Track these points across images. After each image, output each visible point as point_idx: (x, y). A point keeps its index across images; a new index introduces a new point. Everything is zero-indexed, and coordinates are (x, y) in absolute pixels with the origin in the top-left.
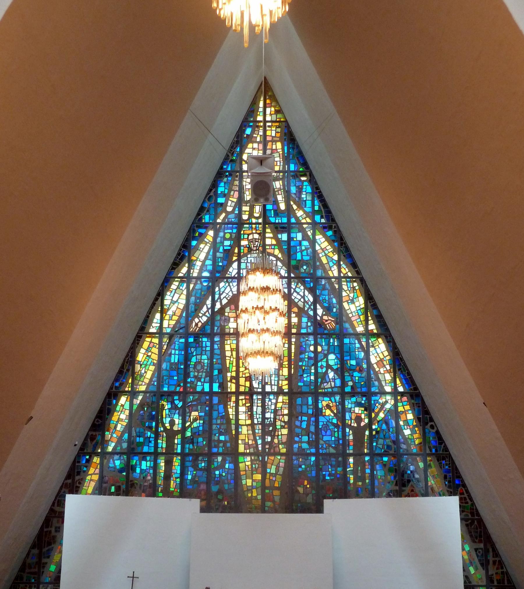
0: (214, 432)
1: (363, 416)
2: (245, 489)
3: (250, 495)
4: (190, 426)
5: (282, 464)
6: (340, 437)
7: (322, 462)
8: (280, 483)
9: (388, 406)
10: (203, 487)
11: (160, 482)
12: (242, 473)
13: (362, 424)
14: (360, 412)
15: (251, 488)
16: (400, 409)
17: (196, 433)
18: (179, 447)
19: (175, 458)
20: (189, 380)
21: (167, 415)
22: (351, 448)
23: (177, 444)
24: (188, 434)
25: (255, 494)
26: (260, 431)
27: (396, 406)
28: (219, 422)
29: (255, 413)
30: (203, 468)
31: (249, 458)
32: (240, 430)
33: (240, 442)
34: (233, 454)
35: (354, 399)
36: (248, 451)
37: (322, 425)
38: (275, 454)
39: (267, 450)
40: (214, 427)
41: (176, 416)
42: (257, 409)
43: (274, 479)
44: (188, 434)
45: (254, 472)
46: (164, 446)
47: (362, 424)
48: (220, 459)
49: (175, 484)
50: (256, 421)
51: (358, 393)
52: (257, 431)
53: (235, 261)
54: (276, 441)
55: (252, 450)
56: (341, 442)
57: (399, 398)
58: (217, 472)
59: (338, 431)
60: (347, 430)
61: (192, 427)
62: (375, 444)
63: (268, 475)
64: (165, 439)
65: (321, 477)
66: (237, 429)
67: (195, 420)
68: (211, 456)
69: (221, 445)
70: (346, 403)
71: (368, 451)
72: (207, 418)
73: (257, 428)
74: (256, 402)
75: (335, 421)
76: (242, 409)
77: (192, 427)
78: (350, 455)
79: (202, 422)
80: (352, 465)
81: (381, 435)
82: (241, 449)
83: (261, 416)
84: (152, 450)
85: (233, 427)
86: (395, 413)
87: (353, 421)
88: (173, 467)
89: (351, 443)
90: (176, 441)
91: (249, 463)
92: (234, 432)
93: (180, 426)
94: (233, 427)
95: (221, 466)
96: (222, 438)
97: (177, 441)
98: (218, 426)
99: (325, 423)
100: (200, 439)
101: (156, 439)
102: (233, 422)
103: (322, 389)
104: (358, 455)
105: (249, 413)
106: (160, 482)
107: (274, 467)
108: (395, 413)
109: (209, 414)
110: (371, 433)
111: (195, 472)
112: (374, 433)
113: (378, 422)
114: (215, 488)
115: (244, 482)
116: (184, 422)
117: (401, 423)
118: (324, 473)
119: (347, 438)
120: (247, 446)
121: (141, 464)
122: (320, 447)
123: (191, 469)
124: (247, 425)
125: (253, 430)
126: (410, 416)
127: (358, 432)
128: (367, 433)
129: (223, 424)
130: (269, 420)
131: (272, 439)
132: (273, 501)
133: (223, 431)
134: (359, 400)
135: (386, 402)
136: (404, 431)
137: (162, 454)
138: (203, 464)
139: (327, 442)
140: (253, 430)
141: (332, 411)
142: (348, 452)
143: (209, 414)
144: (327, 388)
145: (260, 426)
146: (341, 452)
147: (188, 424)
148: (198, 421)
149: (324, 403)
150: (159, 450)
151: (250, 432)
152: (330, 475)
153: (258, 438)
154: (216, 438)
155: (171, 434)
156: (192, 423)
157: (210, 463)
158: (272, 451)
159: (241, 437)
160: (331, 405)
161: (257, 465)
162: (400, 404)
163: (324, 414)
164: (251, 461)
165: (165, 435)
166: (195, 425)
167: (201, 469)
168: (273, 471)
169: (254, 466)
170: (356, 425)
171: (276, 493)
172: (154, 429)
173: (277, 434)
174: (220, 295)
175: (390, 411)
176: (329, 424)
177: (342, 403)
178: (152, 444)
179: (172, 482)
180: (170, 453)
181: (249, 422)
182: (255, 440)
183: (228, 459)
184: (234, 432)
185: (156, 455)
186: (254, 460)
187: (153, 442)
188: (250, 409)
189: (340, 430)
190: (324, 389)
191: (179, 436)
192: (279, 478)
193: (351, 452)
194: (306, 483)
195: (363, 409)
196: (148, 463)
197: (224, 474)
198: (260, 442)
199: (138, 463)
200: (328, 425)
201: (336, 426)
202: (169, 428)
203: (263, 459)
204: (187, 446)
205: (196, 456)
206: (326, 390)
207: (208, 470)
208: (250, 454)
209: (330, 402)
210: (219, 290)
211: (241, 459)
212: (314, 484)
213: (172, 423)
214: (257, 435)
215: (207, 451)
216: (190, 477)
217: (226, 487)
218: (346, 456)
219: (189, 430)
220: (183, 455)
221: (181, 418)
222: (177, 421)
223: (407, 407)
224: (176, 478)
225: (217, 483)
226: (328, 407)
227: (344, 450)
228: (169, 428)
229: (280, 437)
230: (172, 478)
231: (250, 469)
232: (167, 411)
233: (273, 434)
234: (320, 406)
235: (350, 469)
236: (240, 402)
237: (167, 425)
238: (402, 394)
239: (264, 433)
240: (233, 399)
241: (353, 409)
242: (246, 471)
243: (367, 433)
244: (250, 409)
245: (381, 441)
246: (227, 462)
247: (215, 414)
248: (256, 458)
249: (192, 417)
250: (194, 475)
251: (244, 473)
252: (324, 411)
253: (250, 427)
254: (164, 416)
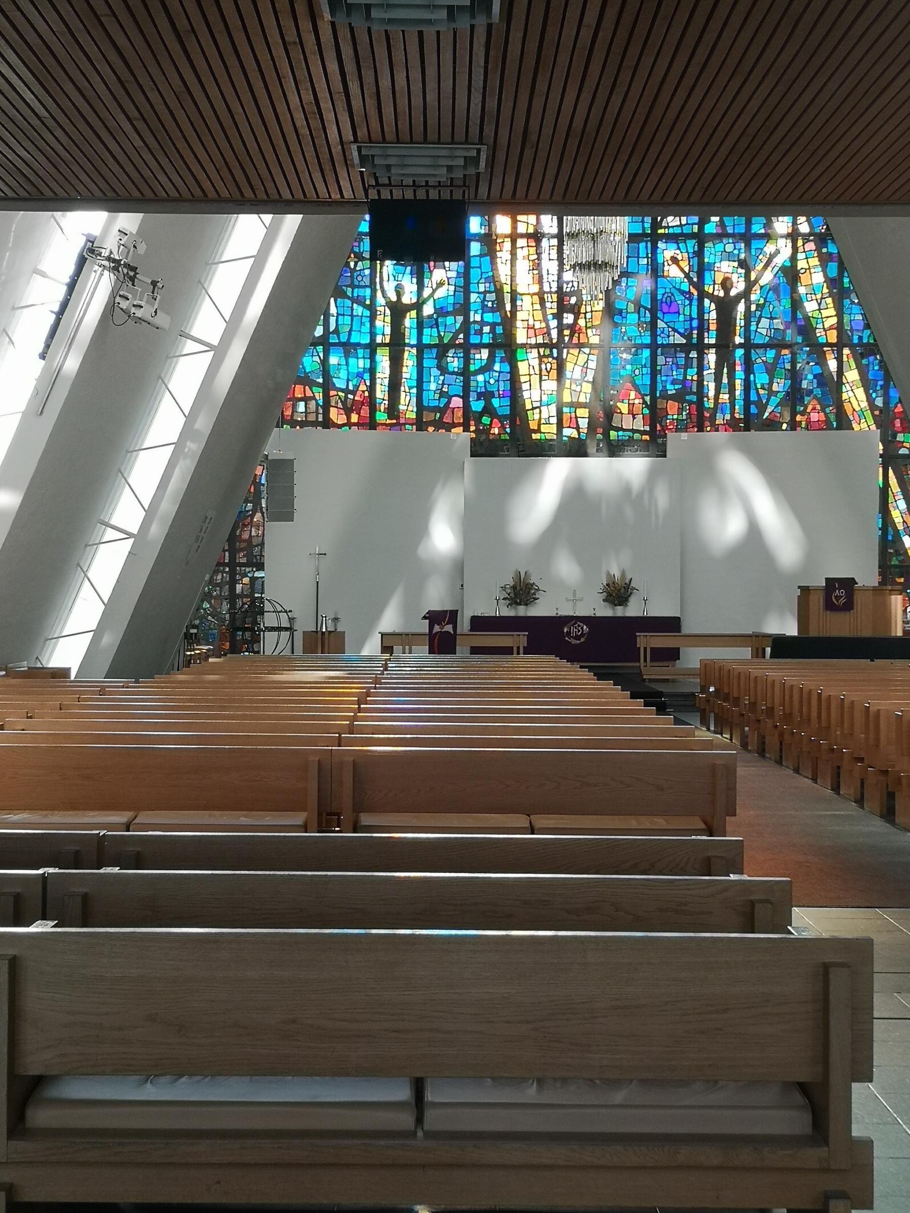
0: (473, 307)
1: (734, 278)
2: (528, 406)
3: (537, 417)
4: (432, 295)
5: (592, 365)
6: (695, 315)
7: (661, 360)
8: (588, 396)
9: (779, 261)
10: (457, 402)
11: (381, 392)
12: (523, 379)
13: (733, 293)
14: (730, 270)
15: (538, 404)
16: (802, 264)
17: (441, 312)
18: (414, 332)
19: (406, 354)
21: (392, 278)
22: (713, 334)
23: (411, 328)
24: (428, 309)
25: (545, 415)
26: (555, 305)
27: (793, 258)
28: (482, 289)
29: (544, 273)
30: (456, 370)
31: (535, 351)
32: (519, 303)
33: (519, 324)
34: (506, 346)
35: (719, 247)
36: (533, 341)
37: (664, 294)
38: (580, 346)
39: (567, 339)
40: (473, 297)
41: (407, 277)
42: (550, 266)
43: (578, 389)
44: (428, 309)
45: (544, 378)
46: (388, 330)
47: (733, 293)
48: (485, 354)
49: (408, 398)
50: (546, 288)
51: (728, 235)
52: (548, 305)
54: (581, 322)
55: (540, 340)
56: (695, 324)
57: (800, 243)
58: (480, 378)
59: (690, 305)
60: (707, 302)
62: (753, 328)
63: (568, 382)
64: (388, 319)
65: (660, 387)
66: (513, 301)
67: (440, 284)
68: (467, 349)
69: (486, 329)
70: (707, 254)
71: (742, 341)
72: (461, 282)
73: (550, 300)
74: (547, 252)
75: (685, 287)
76: (523, 266)
78: (710, 346)
79: (452, 288)
80: (713, 365)
81: (766, 312)
82: (521, 337)
83: (556, 278)
84: (366, 340)
85: (507, 298)
86: (791, 274)
87: (716, 287)
88: (404, 369)
89: (713, 327)
91: (535, 363)
92: (508, 307)
94: (507, 298)
95: (487, 368)
96: (489, 317)
97: (410, 321)
98: (482, 296)
99: (668, 290)
100: (450, 320)
101: (373, 318)
102: (507, 288)
103: (665, 228)
104: (724, 347)
105: (536, 272)
106: (381, 392)
107: (578, 370)
108: (791, 274)
109: (466, 275)
110: (748, 308)
111: (442, 378)
112: (753, 308)
113: (761, 287)
114: (477, 406)
115: (526, 395)
117: (802, 290)
118: (664, 378)
119: (706, 317)
120: (531, 332)
121: (347, 364)
122: (659, 333)
123: (435, 372)
124: (532, 295)
125: (542, 302)
126: (818, 278)
127: (725, 307)
128: (741, 307)
129: (490, 292)
130: (570, 285)
131: (576, 319)
132: (578, 428)
133: (490, 304)
134: (729, 248)
135: (778, 252)
136: (806, 304)
137: (383, 345)
138: (456, 364)
139: (671, 325)
140: (542, 302)
141: (682, 270)
142: (706, 341)
143: (466, 275)
144: (673, 227)
145: (555, 296)
146: (695, 341)
147: (427, 292)
148: (446, 287)
149: (668, 254)
150: (379, 340)
151: (538, 307)
152: (674, 382)
153: (550, 317)
154: (478, 318)
155: (398, 311)
156: (434, 291)
157: (467, 360)
158: (575, 340)
159: (520, 315)
160: (680, 257)
161: (549, 366)
162: (801, 256)
163: (666, 274)
164: (540, 357)
165: (388, 312)
166: (441, 293)
167: (453, 373)
168: (577, 374)
169: (543, 366)
170: (722, 294)
171: (583, 412)
172: (368, 302)
173: (583, 310)
175: (783, 269)
176: (676, 293)
177: (700, 253)
178: (366, 328)
179: (403, 395)
180: (396, 346)
181: (535, 288)
182: (545, 319)
183: (500, 354)
184: (508, 307)
185: (372, 347)
186: (544, 356)
187: (368, 325)
188: (537, 265)
189: (695, 303)
190: (668, 227)
191: (413, 313)
192: (587, 388)
193: (713, 341)
194: (633, 395)
195: (736, 264)
196: (361, 362)
197: (492, 381)
198: (553, 323)
199: (343, 362)
200: (673, 294)
201: (688, 295)
203: (560, 353)
204: (426, 331)
205: (442, 349)
206: (671, 231)
207: (465, 373)
208: (538, 346)
209: (678, 252)
211: (520, 354)
212: (648, 399)
213: (399, 291)
214: (549, 311)
215: (462, 341)
216: (433, 386)
217: (496, 402)
218: (702, 348)
219: (431, 301)
220: (421, 348)
221: (415, 280)
223: (815, 261)
224: (410, 388)
225: (480, 396)
226: (674, 260)
227: (701, 337)
229: (589, 315)
230: (402, 389)
231: (538, 372)
233: (576, 311)
234: (660, 260)
235: (710, 371)
236: (519, 251)
238: (806, 238)
239: (562, 308)
240: (507, 245)
241: (717, 265)
242: (530, 375)
243: (741, 307)
244: (537, 265)
245: (765, 322)
246: (498, 359)
247: (474, 274)
248: (548, 352)
250: (440, 382)
251: (527, 378)
252: (666, 268)
253: (536, 298)
254: (385, 278)
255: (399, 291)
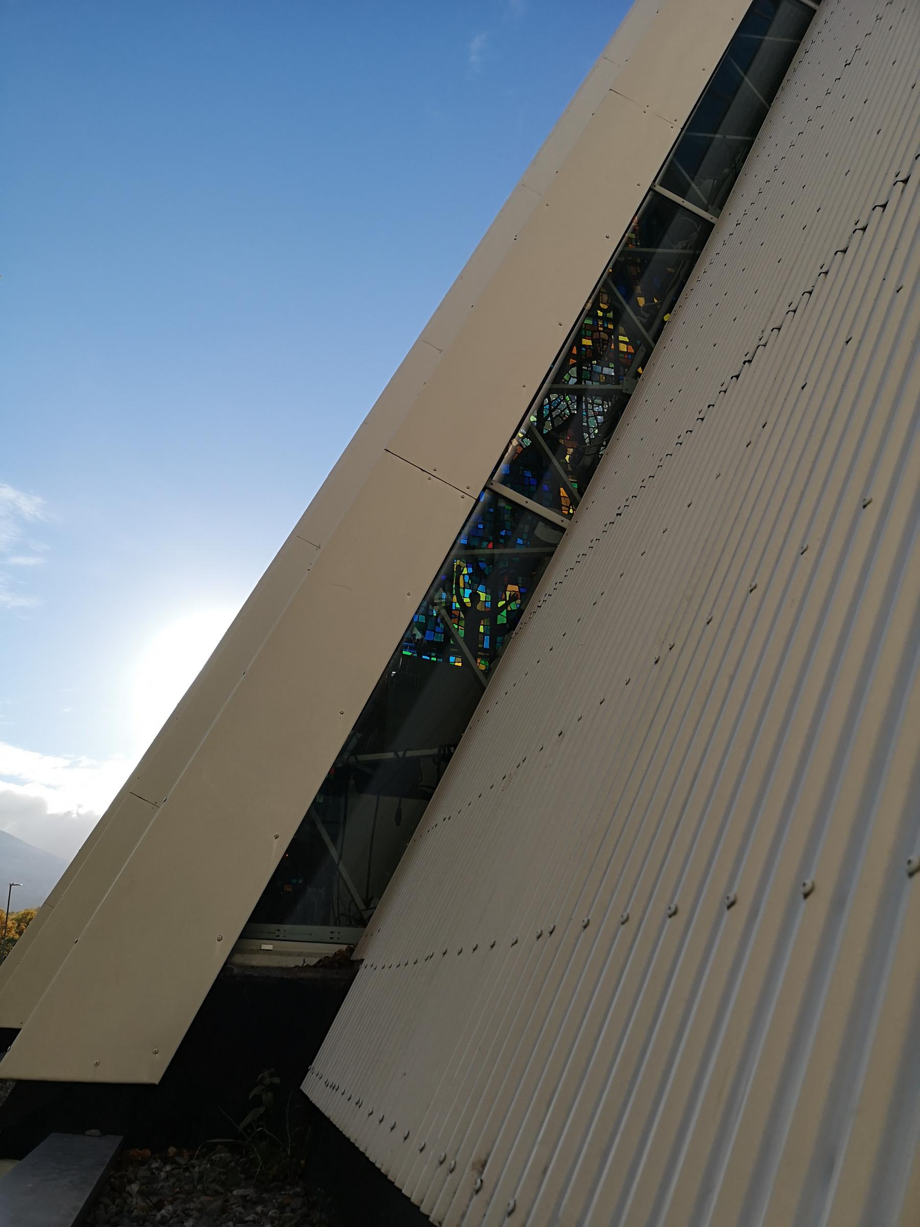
18: (487, 638)
20: (503, 533)
23: (484, 634)
53: (573, 365)
61: (509, 609)
64: (463, 623)
67: (513, 598)
77: (509, 609)
90: (482, 629)
93: (488, 605)
116: (494, 602)
165: (462, 616)
174: (551, 411)
202: (469, 605)
210: (550, 402)
213: (474, 597)
219: (504, 613)
222: (483, 596)
228: (469, 605)
232: (467, 578)
237: (467, 600)
249: (508, 593)
254: (462, 585)
255: (474, 597)
